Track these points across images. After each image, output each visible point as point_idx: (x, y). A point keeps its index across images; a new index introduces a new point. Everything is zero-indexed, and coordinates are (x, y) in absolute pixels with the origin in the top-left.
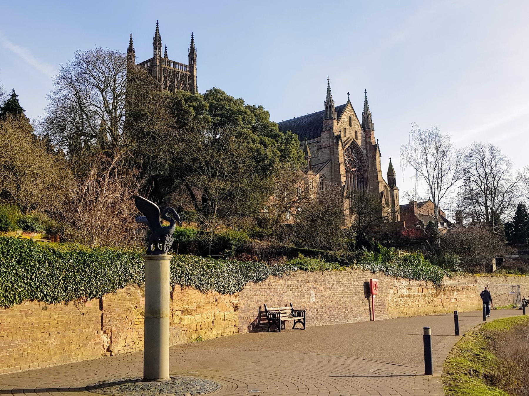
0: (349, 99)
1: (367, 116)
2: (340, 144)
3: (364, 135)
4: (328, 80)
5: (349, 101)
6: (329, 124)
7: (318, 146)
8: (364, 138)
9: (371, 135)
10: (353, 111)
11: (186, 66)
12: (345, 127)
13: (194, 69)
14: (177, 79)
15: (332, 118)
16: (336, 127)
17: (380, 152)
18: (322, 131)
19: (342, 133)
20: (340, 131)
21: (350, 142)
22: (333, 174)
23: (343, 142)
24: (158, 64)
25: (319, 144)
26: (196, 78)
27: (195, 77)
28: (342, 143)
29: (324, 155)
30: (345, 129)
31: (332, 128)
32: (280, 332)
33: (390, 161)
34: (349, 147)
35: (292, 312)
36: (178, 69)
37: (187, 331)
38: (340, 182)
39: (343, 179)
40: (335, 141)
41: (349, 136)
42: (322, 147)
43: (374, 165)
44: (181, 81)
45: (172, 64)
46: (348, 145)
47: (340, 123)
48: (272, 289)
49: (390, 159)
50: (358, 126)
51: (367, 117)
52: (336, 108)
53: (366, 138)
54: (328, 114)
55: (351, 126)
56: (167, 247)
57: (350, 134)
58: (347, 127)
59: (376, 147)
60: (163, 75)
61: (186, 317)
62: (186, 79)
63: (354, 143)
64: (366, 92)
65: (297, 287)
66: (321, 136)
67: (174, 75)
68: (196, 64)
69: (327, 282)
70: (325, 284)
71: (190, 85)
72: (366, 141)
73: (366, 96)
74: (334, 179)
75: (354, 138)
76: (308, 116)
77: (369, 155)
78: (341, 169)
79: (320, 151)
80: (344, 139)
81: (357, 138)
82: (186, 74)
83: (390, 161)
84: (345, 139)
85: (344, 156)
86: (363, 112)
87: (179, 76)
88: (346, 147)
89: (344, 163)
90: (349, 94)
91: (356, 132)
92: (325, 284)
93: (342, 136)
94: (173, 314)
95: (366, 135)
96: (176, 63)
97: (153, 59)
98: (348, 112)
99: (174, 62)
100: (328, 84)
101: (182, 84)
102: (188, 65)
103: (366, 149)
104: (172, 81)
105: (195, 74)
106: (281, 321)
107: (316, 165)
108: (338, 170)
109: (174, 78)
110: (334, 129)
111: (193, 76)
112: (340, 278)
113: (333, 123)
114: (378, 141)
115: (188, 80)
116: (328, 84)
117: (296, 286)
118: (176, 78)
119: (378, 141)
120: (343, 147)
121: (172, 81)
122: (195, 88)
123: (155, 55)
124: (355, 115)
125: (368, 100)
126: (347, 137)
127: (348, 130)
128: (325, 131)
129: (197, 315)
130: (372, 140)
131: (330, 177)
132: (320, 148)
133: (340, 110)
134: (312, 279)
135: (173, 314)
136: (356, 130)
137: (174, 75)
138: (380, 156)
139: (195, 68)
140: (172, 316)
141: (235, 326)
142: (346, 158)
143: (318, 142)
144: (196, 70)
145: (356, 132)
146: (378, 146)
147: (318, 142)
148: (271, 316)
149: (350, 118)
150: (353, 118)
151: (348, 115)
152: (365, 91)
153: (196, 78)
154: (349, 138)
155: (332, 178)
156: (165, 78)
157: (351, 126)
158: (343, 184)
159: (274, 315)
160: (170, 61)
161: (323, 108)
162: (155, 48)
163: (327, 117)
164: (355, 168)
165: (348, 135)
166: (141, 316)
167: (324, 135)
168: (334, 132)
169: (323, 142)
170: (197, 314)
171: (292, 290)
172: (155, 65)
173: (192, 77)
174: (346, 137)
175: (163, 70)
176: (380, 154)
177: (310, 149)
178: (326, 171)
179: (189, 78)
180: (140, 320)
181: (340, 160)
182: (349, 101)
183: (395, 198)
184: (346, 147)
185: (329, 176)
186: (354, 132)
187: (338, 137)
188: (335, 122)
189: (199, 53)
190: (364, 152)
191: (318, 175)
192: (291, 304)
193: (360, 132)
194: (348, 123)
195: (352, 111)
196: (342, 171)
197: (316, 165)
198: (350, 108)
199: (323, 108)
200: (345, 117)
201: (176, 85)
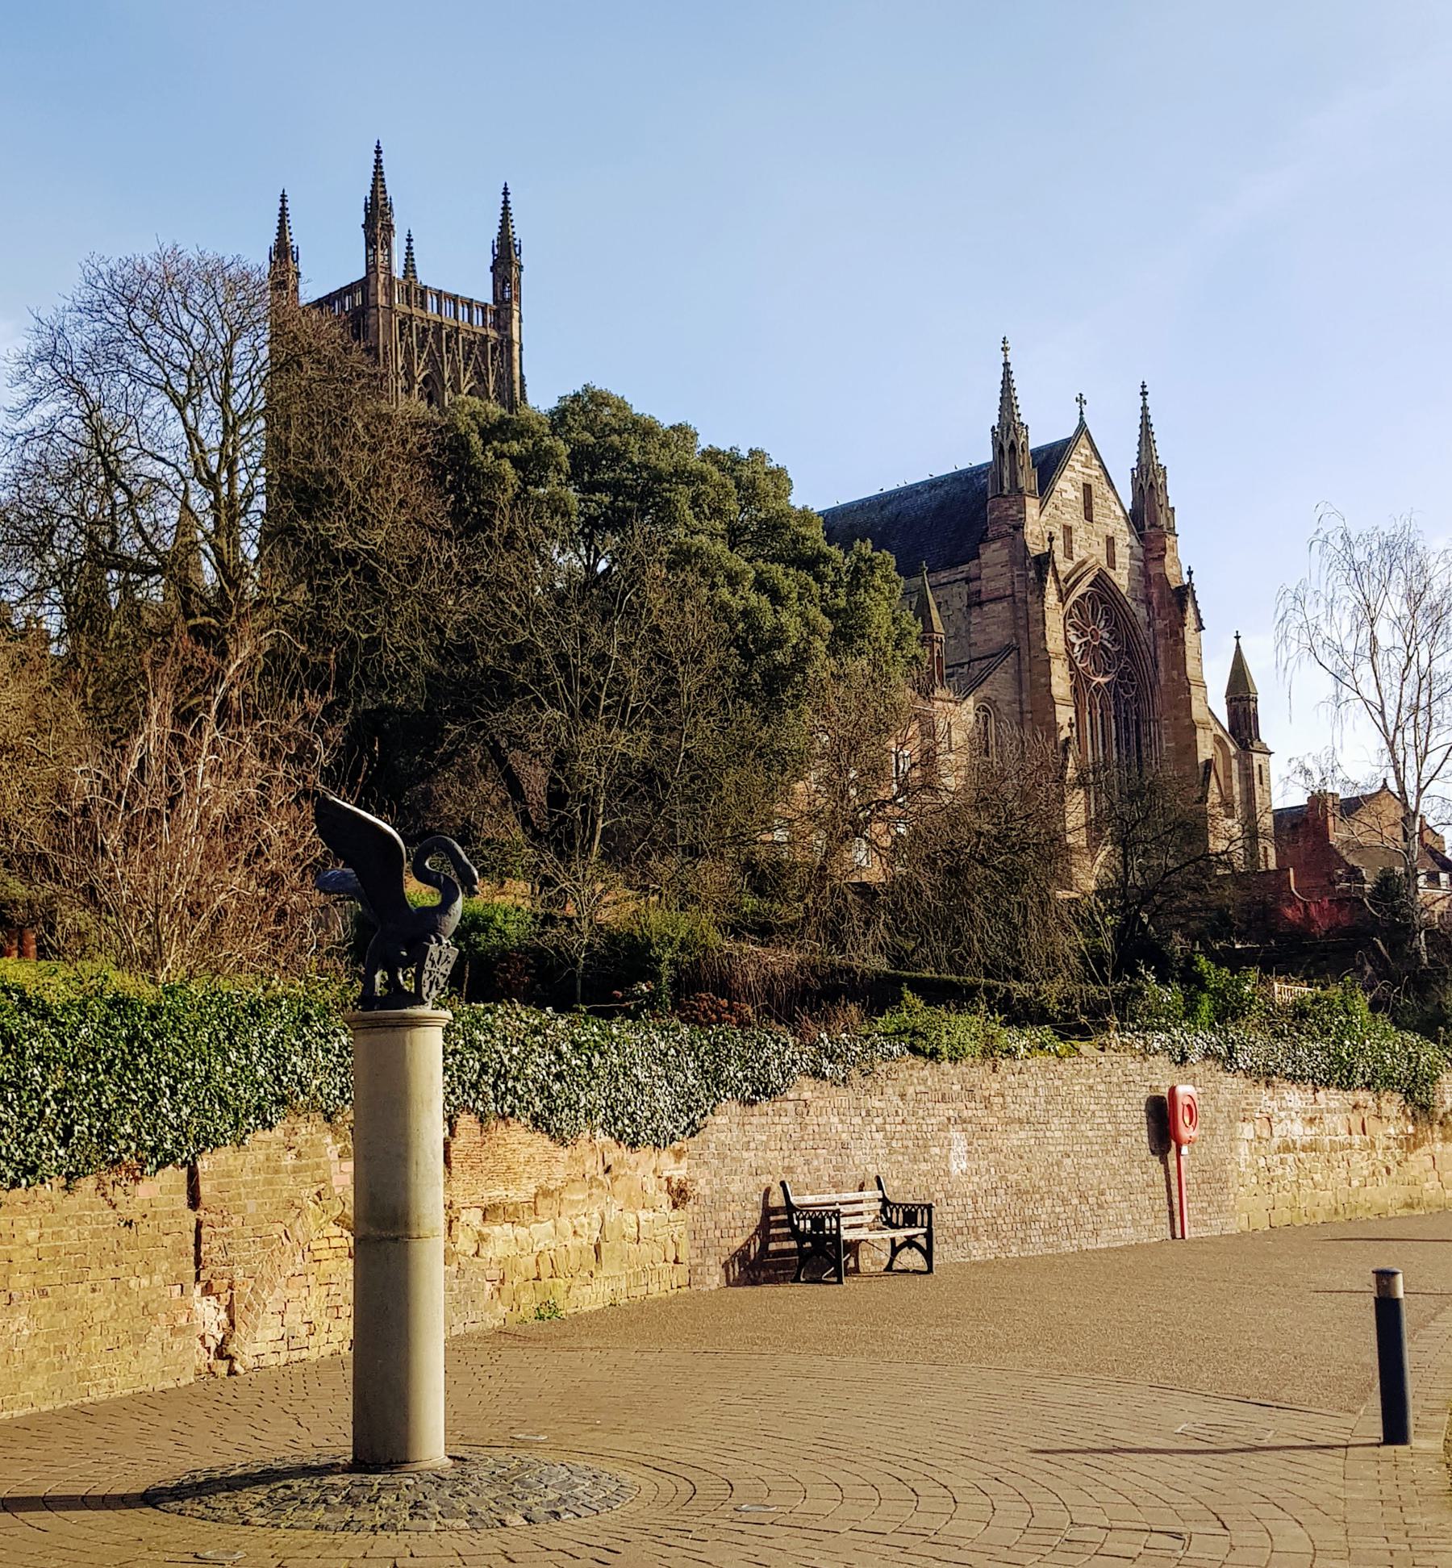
0: (1081, 419)
2: (1051, 588)
3: (1141, 550)
4: (1004, 349)
5: (1082, 428)
6: (1011, 512)
8: (1141, 564)
9: (1164, 549)
10: (1097, 463)
11: (484, 307)
12: (1069, 523)
13: (511, 317)
14: (450, 356)
15: (1020, 491)
16: (1037, 523)
17: (1197, 612)
18: (983, 539)
19: (1058, 544)
20: (1051, 539)
21: (1089, 578)
22: (1024, 696)
23: (1061, 578)
24: (382, 300)
25: (974, 586)
26: (521, 349)
27: (517, 347)
28: (1057, 581)
29: (993, 626)
30: (1068, 530)
31: (1019, 526)
32: (840, 1282)
33: (1238, 646)
34: (1083, 596)
35: (883, 1211)
36: (456, 317)
37: (502, 1281)
38: (1053, 728)
39: (1064, 715)
40: (1032, 574)
41: (1084, 554)
42: (984, 597)
43: (1178, 660)
44: (466, 364)
45: (432, 301)
46: (1081, 589)
47: (1049, 509)
48: (810, 1128)
49: (1237, 637)
50: (1117, 518)
51: (1151, 485)
52: (1036, 453)
53: (1146, 562)
54: (1006, 474)
55: (1089, 518)
56: (431, 983)
57: (1088, 548)
58: (1075, 524)
59: (1183, 595)
60: (401, 340)
61: (500, 1232)
62: (484, 354)
63: (1102, 582)
64: (1144, 394)
65: (899, 1119)
66: (978, 557)
67: (439, 341)
68: (519, 298)
69: (1009, 1099)
70: (1004, 1107)
71: (499, 379)
72: (1145, 573)
73: (1145, 408)
74: (1029, 716)
75: (1104, 563)
76: (933, 484)
77: (1159, 624)
78: (1053, 682)
79: (976, 611)
80: (1064, 566)
82: (485, 338)
83: (1238, 646)
84: (1070, 565)
85: (1066, 631)
86: (1135, 465)
87: (457, 343)
88: (1073, 597)
89: (1065, 656)
90: (1081, 400)
91: (1110, 541)
92: (1004, 1107)
93: (1059, 555)
94: (451, 1222)
95: (1147, 550)
96: (447, 296)
97: (364, 285)
98: (1078, 467)
99: (439, 294)
100: (1006, 364)
101: (468, 375)
102: (491, 302)
103: (1148, 602)
104: (434, 363)
105: (516, 337)
106: (845, 1241)
107: (961, 665)
108: (1043, 680)
109: (440, 352)
110: (1028, 529)
111: (511, 342)
112: (1058, 1083)
113: (1022, 510)
114: (1190, 573)
115: (492, 360)
116: (1006, 364)
117: (897, 1115)
118: (448, 352)
119: (1190, 573)
120: (1062, 598)
121: (434, 363)
122: (517, 386)
123: (371, 267)
124: (1104, 478)
126: (1077, 559)
127: (1079, 535)
128: (993, 540)
129: (537, 1222)
130: (1171, 571)
131: (1016, 706)
132: (976, 602)
133: (1051, 461)
134: (957, 1087)
135: (451, 1222)
136: (1111, 535)
137: (439, 341)
138: (1201, 628)
139: (516, 314)
140: (450, 1228)
141: (676, 1262)
142: (1073, 639)
143: (968, 580)
144: (520, 320)
145: (1110, 541)
146: (1194, 592)
147: (967, 580)
148: (809, 1225)
149: (1087, 488)
150: (1100, 488)
151: (1081, 479)
152: (1143, 386)
153: (521, 349)
154: (1084, 563)
155: (1021, 713)
156: (408, 352)
157: (1089, 518)
158: (1063, 735)
159: (818, 1223)
160: (423, 291)
161: (984, 455)
162: (370, 243)
163: (1002, 488)
164: (1106, 673)
165: (1079, 553)
166: (337, 1231)
167: (993, 554)
168: (1029, 540)
169: (989, 580)
170: (539, 1218)
171: (884, 1130)
172: (371, 304)
173: (506, 345)
175: (402, 323)
176: (1199, 620)
177: (939, 605)
178: (999, 684)
179: (494, 349)
180: (335, 1242)
181: (1050, 646)
182: (1082, 428)
183: (1257, 781)
184: (1073, 597)
185: (1009, 704)
187: (1044, 562)
188: (1032, 506)
189: (528, 255)
190: (1142, 613)
191: (970, 701)
192: (878, 1179)
193: (1125, 541)
194: (1081, 507)
195: (1095, 462)
196: (1060, 683)
197: (961, 665)
198: (1088, 452)
199: (984, 455)
200: (1067, 487)
201: (446, 376)
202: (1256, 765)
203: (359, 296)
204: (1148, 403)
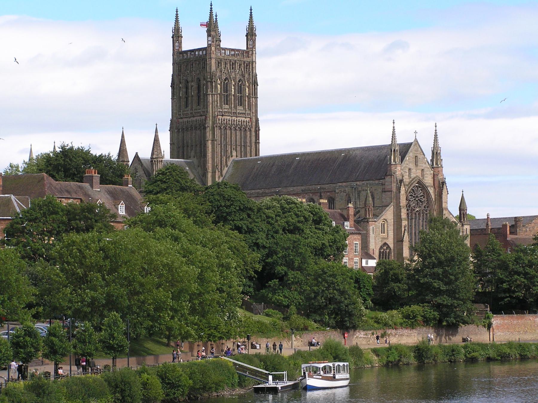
1: (436, 153)
4: (394, 123)
5: (416, 140)
7: (383, 189)
27: (254, 63)
55: (416, 165)
57: (416, 173)
66: (384, 179)
78: (402, 214)
81: (423, 175)
83: (463, 194)
100: (394, 127)
107: (380, 207)
116: (394, 127)
125: (437, 134)
127: (413, 171)
128: (389, 175)
136: (423, 168)
150: (420, 156)
154: (414, 178)
169: (387, 185)
174: (411, 177)
186: (420, 171)
196: (404, 213)
197: (380, 207)
199: (390, 143)
202: (465, 229)
203: (204, 52)
204: (437, 129)
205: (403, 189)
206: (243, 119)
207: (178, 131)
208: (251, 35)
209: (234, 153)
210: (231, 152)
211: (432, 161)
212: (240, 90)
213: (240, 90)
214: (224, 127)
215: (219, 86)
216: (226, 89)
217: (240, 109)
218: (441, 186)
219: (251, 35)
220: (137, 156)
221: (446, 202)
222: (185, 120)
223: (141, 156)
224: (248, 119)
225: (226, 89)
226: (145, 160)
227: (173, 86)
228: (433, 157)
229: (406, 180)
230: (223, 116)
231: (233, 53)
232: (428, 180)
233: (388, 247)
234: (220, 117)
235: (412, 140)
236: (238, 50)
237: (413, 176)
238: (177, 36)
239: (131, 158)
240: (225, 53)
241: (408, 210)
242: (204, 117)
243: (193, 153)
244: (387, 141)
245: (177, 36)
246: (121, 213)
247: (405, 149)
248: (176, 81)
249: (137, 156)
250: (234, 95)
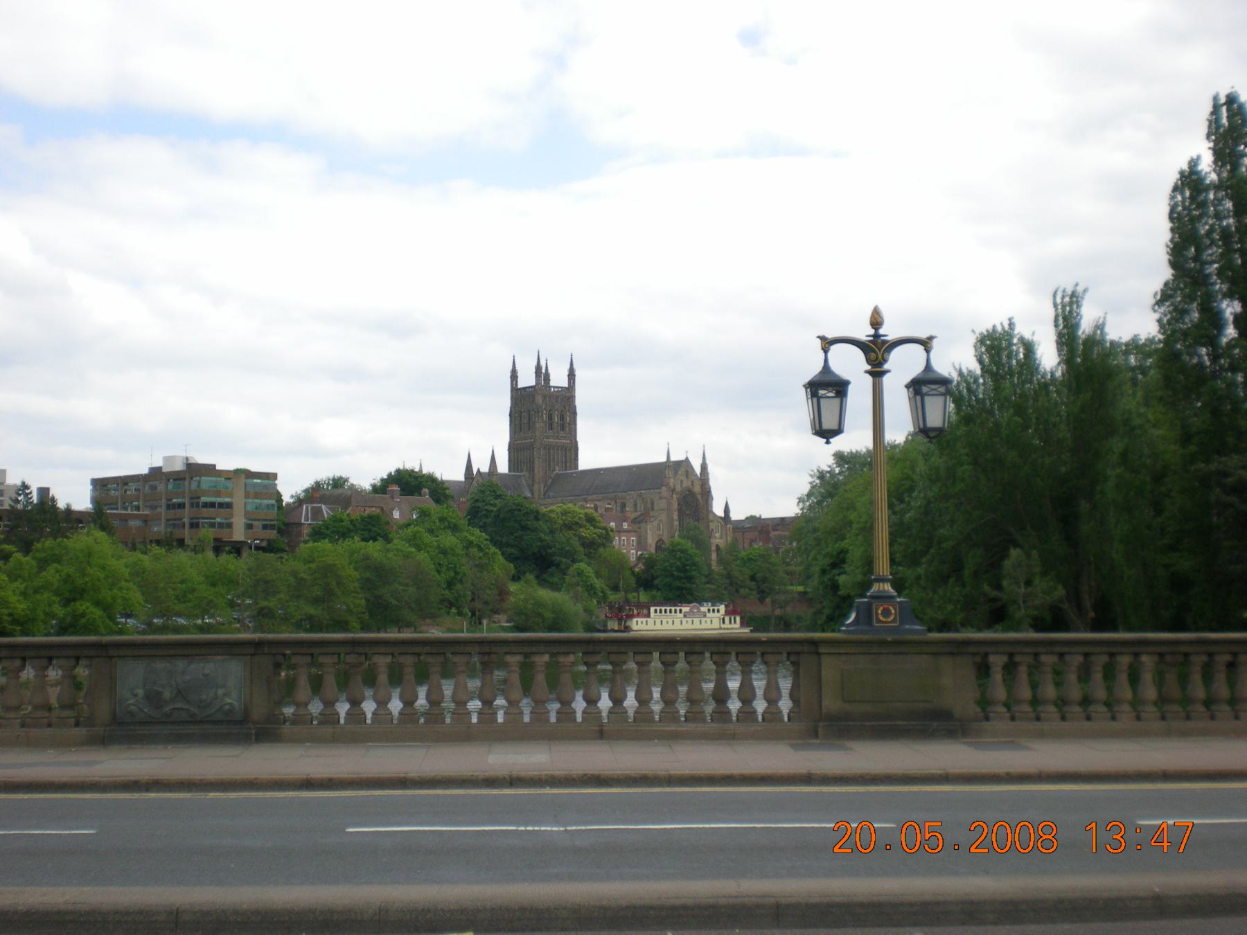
1: (704, 467)
5: (687, 458)
18: (662, 486)
30: (682, 481)
55: (687, 477)
57: (686, 484)
63: (690, 491)
90: (687, 452)
91: (692, 482)
127: (685, 482)
130: (707, 486)
145: (692, 482)
147: (660, 493)
182: (687, 458)
187: (673, 491)
200: (681, 471)
205: (675, 496)
206: (564, 441)
207: (514, 452)
208: (572, 375)
209: (557, 468)
210: (555, 468)
211: (701, 474)
212: (562, 418)
213: (562, 418)
214: (548, 448)
215: (545, 416)
216: (550, 417)
217: (562, 434)
218: (707, 494)
219: (572, 375)
220: (479, 470)
221: (712, 507)
222: (519, 442)
223: (482, 470)
224: (569, 441)
225: (550, 417)
226: (485, 473)
227: (510, 415)
228: (702, 470)
229: (678, 488)
230: (548, 438)
231: (556, 389)
232: (697, 489)
233: (663, 542)
234: (545, 440)
235: (683, 458)
236: (561, 388)
237: (684, 486)
238: (514, 376)
239: (475, 472)
240: (550, 390)
241: (679, 512)
242: (532, 440)
243: (525, 468)
244: (663, 459)
245: (514, 376)
246: (396, 517)
247: (679, 463)
248: (513, 412)
249: (479, 470)
250: (557, 423)
